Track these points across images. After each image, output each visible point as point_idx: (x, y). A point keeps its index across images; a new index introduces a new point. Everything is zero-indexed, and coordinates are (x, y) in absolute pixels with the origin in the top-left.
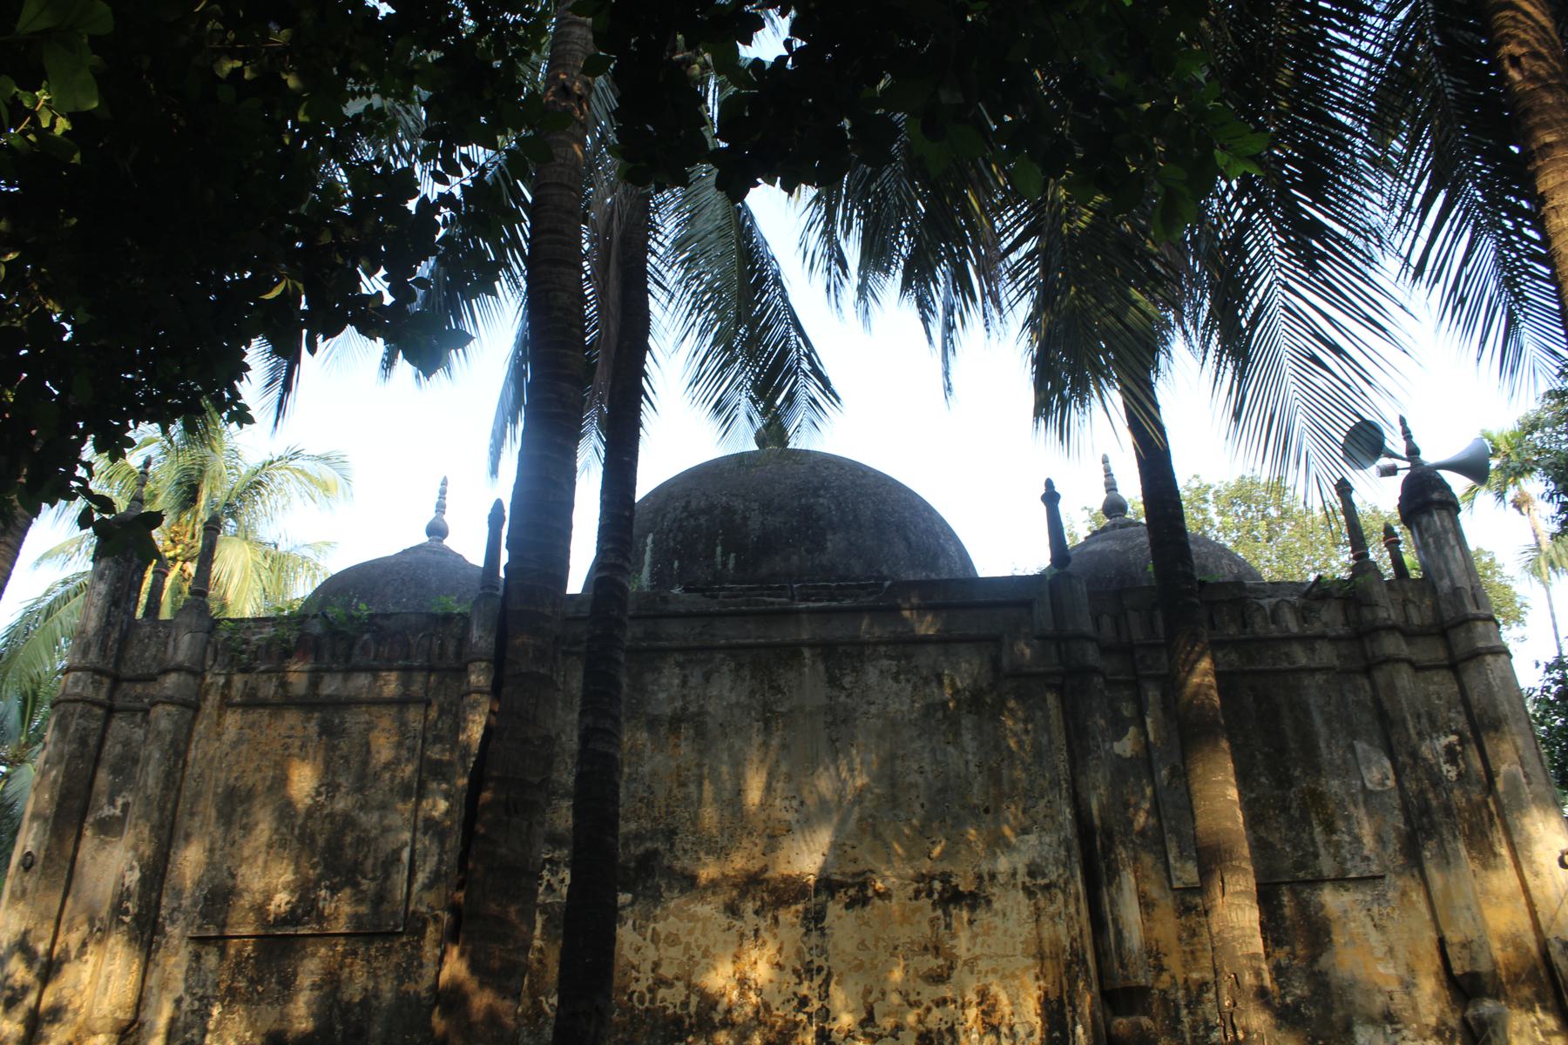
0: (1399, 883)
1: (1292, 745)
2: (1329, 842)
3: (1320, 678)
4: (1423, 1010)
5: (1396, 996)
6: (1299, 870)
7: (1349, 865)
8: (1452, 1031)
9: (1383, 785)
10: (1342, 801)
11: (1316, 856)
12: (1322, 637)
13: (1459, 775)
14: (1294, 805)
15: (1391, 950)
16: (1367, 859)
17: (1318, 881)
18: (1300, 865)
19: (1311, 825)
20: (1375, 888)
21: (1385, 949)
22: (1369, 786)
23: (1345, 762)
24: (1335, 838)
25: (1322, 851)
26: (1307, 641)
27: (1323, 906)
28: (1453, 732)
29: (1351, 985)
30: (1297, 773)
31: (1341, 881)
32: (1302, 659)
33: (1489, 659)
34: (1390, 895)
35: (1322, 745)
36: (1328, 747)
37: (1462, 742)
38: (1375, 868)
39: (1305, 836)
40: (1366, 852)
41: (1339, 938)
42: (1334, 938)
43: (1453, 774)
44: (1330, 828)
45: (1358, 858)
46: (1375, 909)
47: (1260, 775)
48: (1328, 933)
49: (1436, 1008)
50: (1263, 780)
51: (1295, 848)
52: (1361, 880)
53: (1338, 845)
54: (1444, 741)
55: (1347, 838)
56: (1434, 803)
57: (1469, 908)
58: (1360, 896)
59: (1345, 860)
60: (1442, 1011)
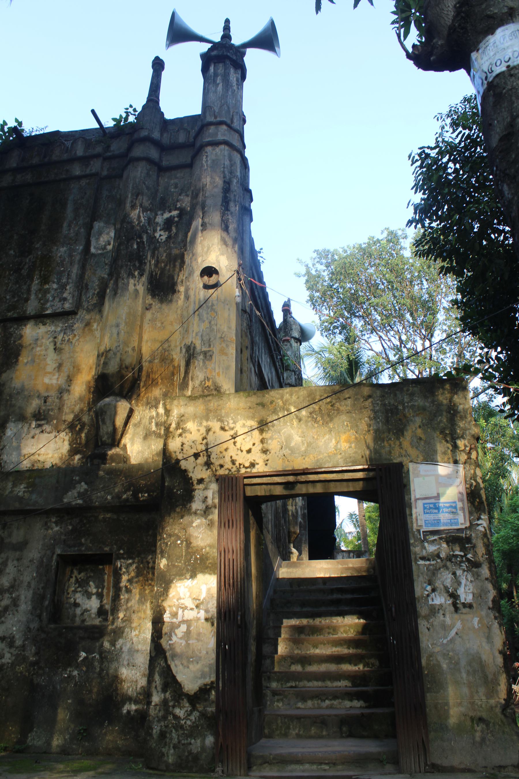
0: (87, 317)
1: (43, 227)
2: (40, 290)
3: (83, 182)
4: (66, 409)
5: (50, 400)
6: (9, 311)
7: (48, 305)
8: (83, 426)
9: (104, 248)
10: (62, 261)
11: (27, 300)
12: (97, 156)
13: (169, 237)
14: (27, 266)
15: (60, 366)
16: (65, 299)
17: (23, 319)
18: (13, 307)
19: (32, 280)
20: (67, 322)
21: (55, 365)
22: (93, 250)
23: (77, 234)
24: (47, 286)
25: (33, 297)
26: (85, 160)
27: (21, 337)
28: (176, 209)
29: (18, 393)
30: (38, 246)
31: (40, 318)
32: (77, 170)
33: (209, 149)
34: (76, 326)
35: (65, 225)
36: (69, 226)
37: (180, 216)
38: (67, 306)
39: (25, 287)
40: (65, 295)
41: (23, 359)
42: (20, 359)
43: (164, 238)
44: (45, 280)
45: (57, 300)
46: (60, 337)
47: (10, 249)
48: (17, 354)
49: (77, 409)
50: (12, 252)
51: (13, 297)
52: (56, 316)
53: (47, 291)
54: (167, 215)
55: (55, 286)
56: (123, 252)
57: (118, 326)
58: (53, 328)
59: (47, 301)
60: (82, 410)
